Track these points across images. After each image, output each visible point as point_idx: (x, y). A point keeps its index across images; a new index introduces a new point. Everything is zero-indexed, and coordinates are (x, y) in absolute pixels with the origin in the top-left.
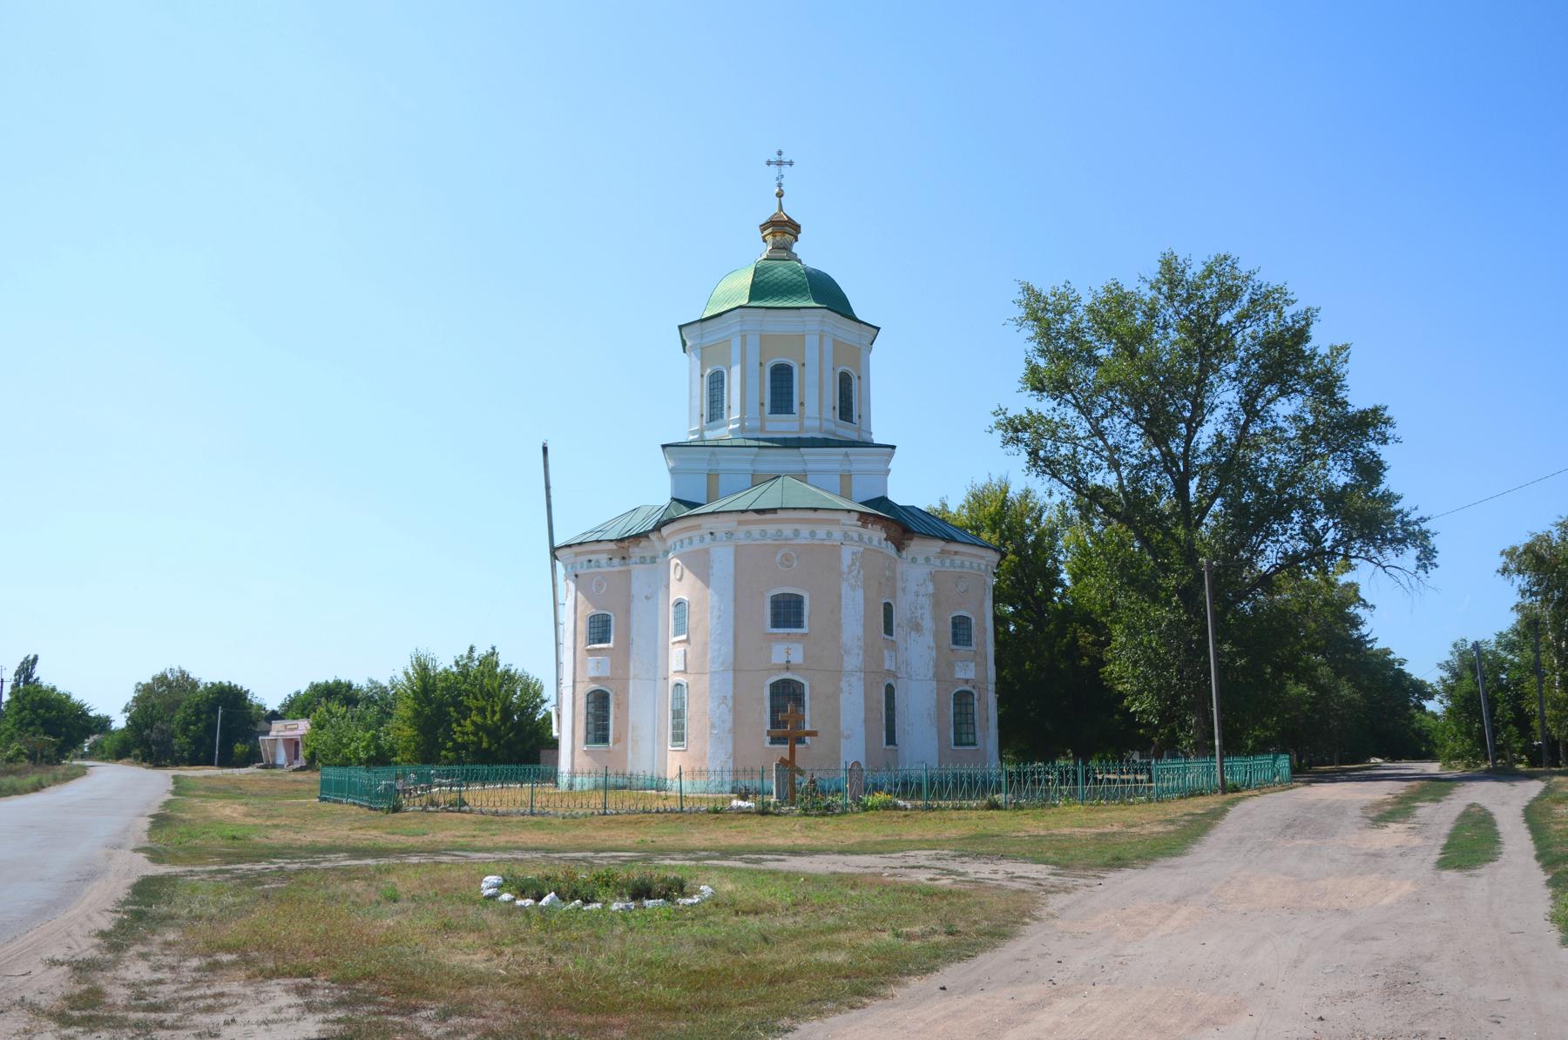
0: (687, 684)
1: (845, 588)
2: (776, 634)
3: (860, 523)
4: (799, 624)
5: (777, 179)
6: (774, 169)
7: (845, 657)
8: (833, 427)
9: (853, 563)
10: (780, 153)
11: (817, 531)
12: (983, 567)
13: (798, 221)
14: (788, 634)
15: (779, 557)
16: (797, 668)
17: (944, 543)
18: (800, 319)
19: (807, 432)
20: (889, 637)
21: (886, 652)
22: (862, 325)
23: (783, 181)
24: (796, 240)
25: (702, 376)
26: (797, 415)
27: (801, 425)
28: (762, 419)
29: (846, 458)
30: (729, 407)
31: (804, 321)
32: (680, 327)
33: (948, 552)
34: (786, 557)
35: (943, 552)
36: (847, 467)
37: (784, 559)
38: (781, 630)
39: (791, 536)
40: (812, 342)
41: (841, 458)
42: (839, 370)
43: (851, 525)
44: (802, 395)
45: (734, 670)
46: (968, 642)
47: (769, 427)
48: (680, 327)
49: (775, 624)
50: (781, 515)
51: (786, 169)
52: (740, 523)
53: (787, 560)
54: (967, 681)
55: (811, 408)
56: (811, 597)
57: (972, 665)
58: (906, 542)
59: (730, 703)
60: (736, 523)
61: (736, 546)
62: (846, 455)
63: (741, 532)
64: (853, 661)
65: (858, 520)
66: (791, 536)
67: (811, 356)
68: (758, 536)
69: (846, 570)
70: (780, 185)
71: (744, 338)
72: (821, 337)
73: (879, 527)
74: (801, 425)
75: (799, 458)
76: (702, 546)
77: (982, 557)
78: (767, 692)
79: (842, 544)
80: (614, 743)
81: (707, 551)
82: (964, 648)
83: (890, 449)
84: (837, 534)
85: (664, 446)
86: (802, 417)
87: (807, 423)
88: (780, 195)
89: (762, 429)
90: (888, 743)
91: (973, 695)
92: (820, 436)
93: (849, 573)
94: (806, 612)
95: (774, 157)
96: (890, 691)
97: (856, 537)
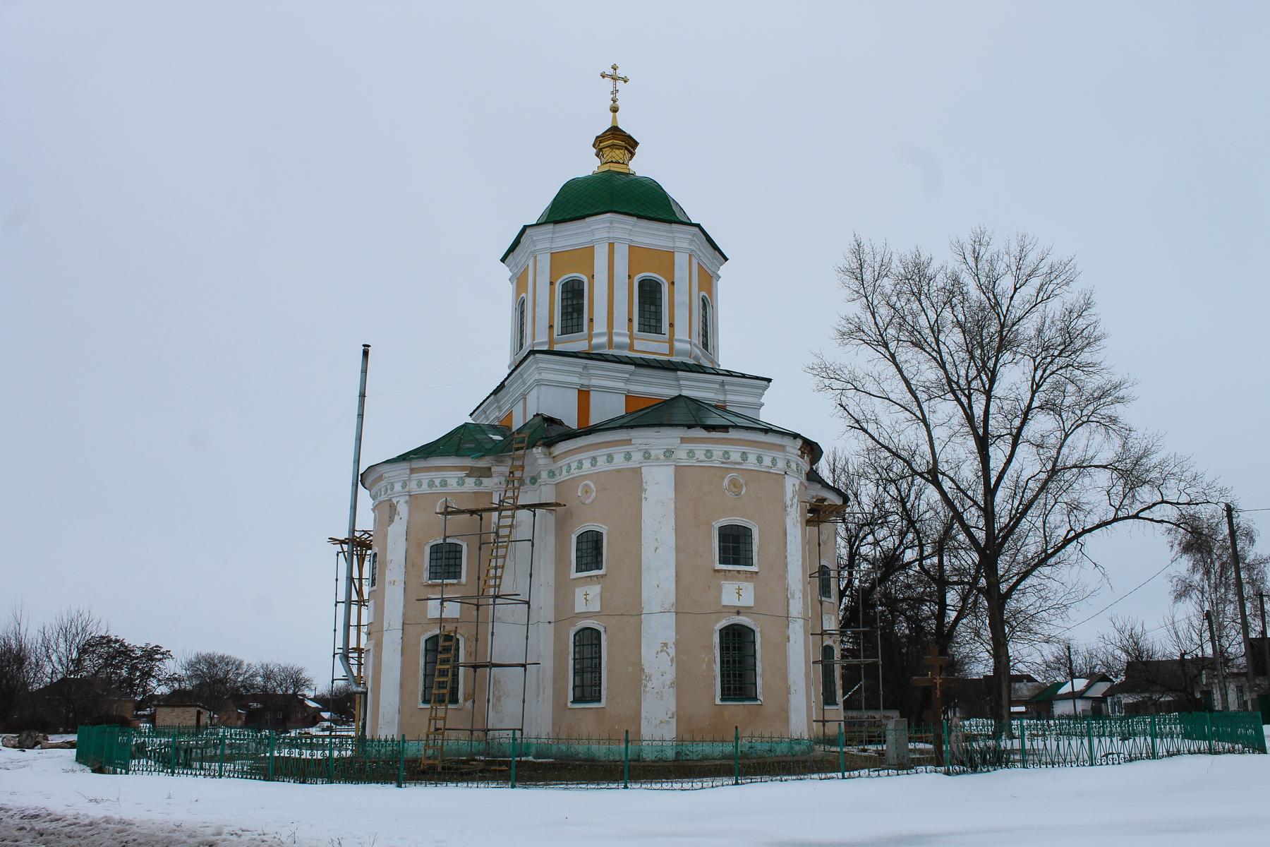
2: (725, 571)
5: (612, 93)
7: (791, 600)
9: (794, 496)
14: (739, 572)
15: (726, 481)
17: (820, 486)
18: (671, 235)
25: (552, 283)
26: (667, 336)
27: (671, 348)
28: (631, 336)
29: (721, 388)
30: (591, 320)
34: (734, 483)
37: (732, 486)
38: (730, 567)
39: (739, 460)
40: (681, 260)
41: (717, 386)
42: (703, 293)
44: (672, 317)
45: (676, 613)
47: (638, 345)
49: (723, 561)
50: (733, 434)
51: (620, 84)
52: (683, 440)
53: (735, 487)
59: (672, 651)
60: (679, 440)
61: (676, 466)
63: (681, 454)
66: (739, 460)
67: (681, 274)
69: (789, 503)
70: (614, 101)
71: (611, 246)
74: (671, 348)
75: (675, 383)
76: (630, 465)
78: (716, 639)
79: (786, 473)
80: (465, 700)
81: (637, 471)
83: (766, 383)
84: (781, 464)
86: (671, 340)
87: (677, 345)
89: (631, 347)
92: (691, 361)
93: (791, 506)
94: (755, 548)
95: (610, 71)
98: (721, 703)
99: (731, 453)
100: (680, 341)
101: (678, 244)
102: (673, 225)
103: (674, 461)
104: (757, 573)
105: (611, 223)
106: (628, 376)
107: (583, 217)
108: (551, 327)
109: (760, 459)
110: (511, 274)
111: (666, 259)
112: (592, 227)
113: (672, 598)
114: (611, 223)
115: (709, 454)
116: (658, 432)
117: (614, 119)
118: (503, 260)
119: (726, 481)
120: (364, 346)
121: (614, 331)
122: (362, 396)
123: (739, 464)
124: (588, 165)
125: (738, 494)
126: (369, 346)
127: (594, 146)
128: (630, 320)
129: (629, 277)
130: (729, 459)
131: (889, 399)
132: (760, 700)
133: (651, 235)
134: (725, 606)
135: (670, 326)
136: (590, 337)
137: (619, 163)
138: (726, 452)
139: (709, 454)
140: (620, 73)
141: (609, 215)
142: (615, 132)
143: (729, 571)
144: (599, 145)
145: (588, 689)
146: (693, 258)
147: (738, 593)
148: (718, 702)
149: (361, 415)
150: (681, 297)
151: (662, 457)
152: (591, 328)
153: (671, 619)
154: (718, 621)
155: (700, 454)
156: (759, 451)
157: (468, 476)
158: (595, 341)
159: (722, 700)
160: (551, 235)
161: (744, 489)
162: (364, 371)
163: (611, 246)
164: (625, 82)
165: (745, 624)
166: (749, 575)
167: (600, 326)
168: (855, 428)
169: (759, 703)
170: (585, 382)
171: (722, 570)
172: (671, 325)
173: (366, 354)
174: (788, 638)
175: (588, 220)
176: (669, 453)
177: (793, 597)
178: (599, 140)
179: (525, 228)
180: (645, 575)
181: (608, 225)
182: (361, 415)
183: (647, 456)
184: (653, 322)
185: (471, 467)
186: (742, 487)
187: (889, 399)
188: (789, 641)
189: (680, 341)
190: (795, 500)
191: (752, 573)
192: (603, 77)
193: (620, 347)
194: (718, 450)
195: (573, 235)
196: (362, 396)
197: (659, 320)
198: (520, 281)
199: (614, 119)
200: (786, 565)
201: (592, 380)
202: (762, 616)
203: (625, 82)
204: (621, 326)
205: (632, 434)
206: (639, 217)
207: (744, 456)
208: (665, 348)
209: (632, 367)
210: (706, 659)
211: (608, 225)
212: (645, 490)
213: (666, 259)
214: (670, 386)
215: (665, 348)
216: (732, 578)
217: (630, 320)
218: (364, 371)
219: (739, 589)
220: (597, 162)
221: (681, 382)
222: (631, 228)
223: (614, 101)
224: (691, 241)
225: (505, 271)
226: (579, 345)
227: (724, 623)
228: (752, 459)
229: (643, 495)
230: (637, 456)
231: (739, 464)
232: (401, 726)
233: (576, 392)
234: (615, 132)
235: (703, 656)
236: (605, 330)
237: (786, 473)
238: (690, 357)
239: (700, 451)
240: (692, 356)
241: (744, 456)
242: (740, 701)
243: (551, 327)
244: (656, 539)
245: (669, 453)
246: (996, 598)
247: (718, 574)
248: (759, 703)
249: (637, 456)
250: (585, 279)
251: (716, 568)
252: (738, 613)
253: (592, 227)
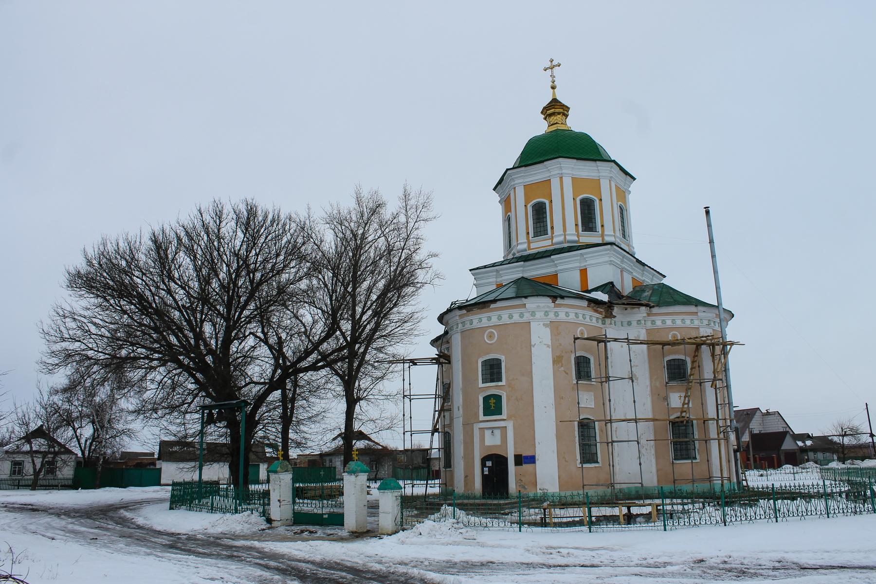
6: (549, 72)
10: (552, 61)
13: (569, 106)
26: (600, 232)
28: (578, 236)
30: (552, 228)
40: (604, 184)
42: (619, 203)
86: (602, 235)
88: (553, 88)
95: (548, 65)
101: (601, 174)
102: (598, 162)
107: (542, 162)
108: (528, 233)
110: (500, 199)
117: (554, 94)
118: (494, 189)
121: (567, 233)
124: (540, 127)
127: (542, 113)
128: (576, 225)
133: (585, 170)
136: (552, 238)
140: (555, 63)
142: (555, 103)
144: (546, 112)
146: (612, 182)
152: (553, 233)
158: (555, 240)
167: (558, 230)
175: (546, 163)
178: (545, 111)
179: (507, 170)
195: (537, 174)
198: (506, 203)
199: (554, 94)
206: (577, 159)
213: (595, 184)
220: (545, 124)
222: (573, 166)
223: (553, 82)
224: (611, 171)
225: (496, 197)
234: (555, 103)
236: (562, 233)
243: (528, 233)
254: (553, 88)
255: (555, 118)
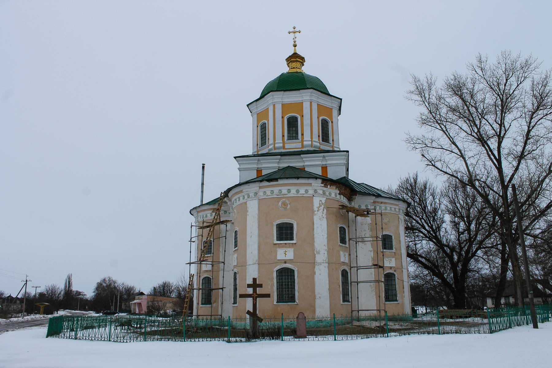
0: (238, 272)
1: (316, 218)
2: (279, 244)
3: (323, 185)
4: (292, 239)
7: (317, 255)
8: (318, 144)
9: (320, 206)
11: (300, 190)
12: (397, 210)
14: (286, 244)
15: (280, 204)
16: (290, 261)
17: (375, 197)
18: (301, 95)
19: (305, 147)
20: (344, 245)
21: (342, 253)
22: (333, 98)
23: (296, 40)
24: (303, 65)
26: (300, 140)
28: (284, 143)
31: (302, 96)
32: (248, 105)
33: (378, 202)
34: (284, 204)
35: (374, 202)
36: (324, 163)
37: (283, 205)
38: (282, 242)
39: (286, 193)
40: (306, 106)
41: (321, 158)
42: (321, 118)
43: (318, 186)
45: (259, 264)
46: (391, 248)
47: (287, 146)
48: (248, 105)
51: (297, 34)
52: (260, 187)
53: (284, 205)
54: (391, 268)
55: (307, 137)
56: (297, 224)
57: (393, 259)
58: (353, 197)
60: (258, 188)
61: (259, 199)
62: (324, 157)
64: (322, 257)
65: (322, 183)
66: (286, 193)
68: (269, 194)
69: (315, 208)
70: (295, 42)
71: (274, 105)
72: (311, 103)
73: (335, 187)
77: (397, 205)
79: (313, 196)
81: (246, 203)
82: (388, 251)
84: (311, 192)
85: (235, 158)
86: (302, 141)
87: (305, 143)
88: (295, 46)
89: (284, 147)
90: (344, 301)
91: (395, 275)
94: (295, 232)
95: (292, 30)
96: (345, 274)
97: (321, 192)
98: (276, 304)
99: (282, 190)
100: (306, 141)
103: (257, 197)
104: (295, 243)
105: (273, 96)
106: (278, 161)
109: (298, 191)
111: (299, 106)
112: (267, 100)
113: (257, 258)
114: (273, 96)
115: (272, 192)
116: (249, 185)
117: (295, 50)
119: (280, 204)
120: (202, 164)
122: (203, 184)
123: (286, 195)
125: (285, 209)
126: (205, 164)
128: (283, 136)
129: (282, 117)
130: (281, 193)
131: (443, 149)
132: (297, 302)
134: (278, 260)
135: (303, 135)
137: (295, 68)
138: (280, 190)
139: (272, 192)
140: (297, 30)
141: (271, 93)
143: (281, 244)
145: (346, 297)
147: (285, 254)
148: (275, 303)
149: (202, 192)
150: (307, 121)
151: (253, 196)
153: (256, 267)
154: (276, 267)
155: (268, 193)
156: (297, 188)
157: (213, 212)
159: (277, 302)
160: (256, 107)
161: (289, 206)
162: (203, 174)
163: (274, 105)
164: (300, 32)
165: (289, 267)
166: (292, 245)
168: (429, 165)
169: (296, 303)
170: (260, 166)
171: (277, 244)
172: (302, 135)
173: (203, 167)
174: (315, 272)
176: (256, 194)
177: (319, 253)
180: (248, 248)
181: (272, 97)
182: (202, 192)
183: (249, 197)
184: (294, 135)
185: (214, 209)
186: (288, 205)
187: (443, 149)
188: (315, 274)
189: (306, 141)
190: (322, 208)
191: (293, 244)
192: (289, 33)
193: (279, 148)
194: (276, 190)
196: (203, 184)
197: (297, 133)
199: (295, 50)
200: (313, 238)
201: (305, 163)
202: (299, 263)
203: (300, 32)
204: (279, 139)
205: (242, 188)
206: (285, 91)
207: (289, 191)
208: (299, 145)
209: (279, 157)
210: (270, 284)
211: (272, 97)
212: (248, 211)
213: (299, 106)
214: (299, 162)
215: (299, 145)
216: (283, 247)
217: (283, 136)
218: (203, 174)
219: (285, 252)
221: (304, 159)
223: (295, 42)
226: (265, 151)
227: (278, 267)
228: (293, 191)
229: (247, 214)
230: (246, 197)
231: (286, 195)
232: (331, 310)
233: (256, 171)
235: (269, 283)
237: (313, 196)
238: (312, 147)
239: (268, 191)
240: (313, 146)
241: (289, 191)
242: (286, 303)
244: (251, 232)
245: (256, 194)
246: (510, 242)
247: (276, 246)
248: (296, 303)
249: (246, 197)
250: (266, 122)
251: (274, 243)
252: (285, 262)
253: (267, 100)
254: (295, 46)
255: (296, 65)
